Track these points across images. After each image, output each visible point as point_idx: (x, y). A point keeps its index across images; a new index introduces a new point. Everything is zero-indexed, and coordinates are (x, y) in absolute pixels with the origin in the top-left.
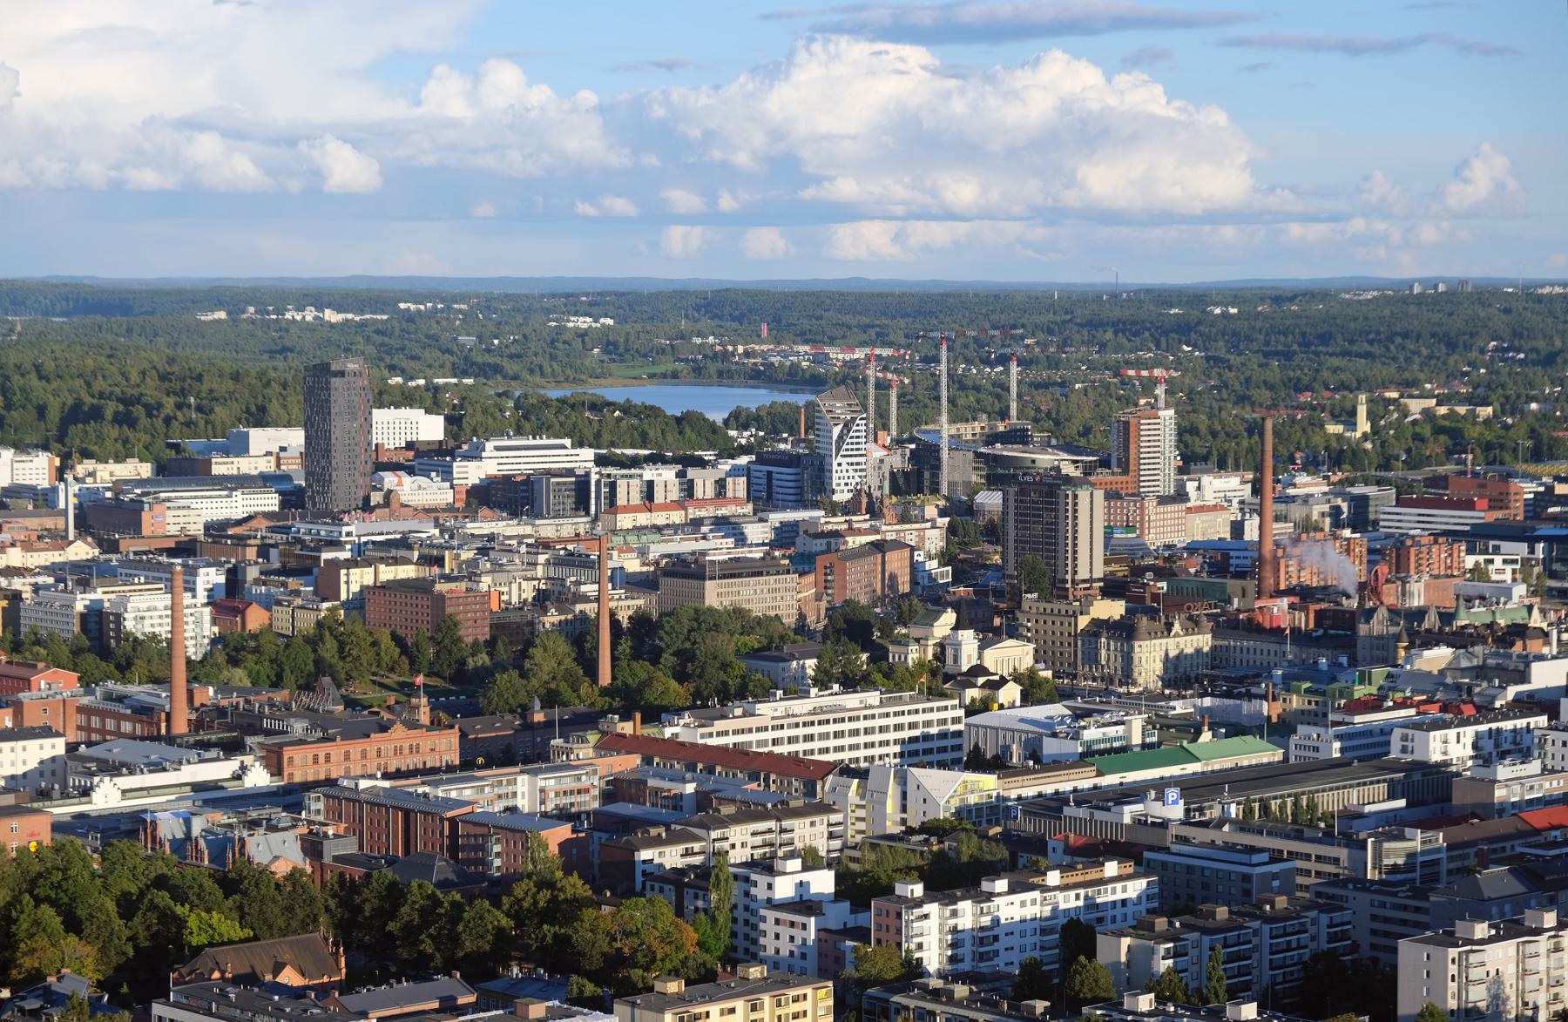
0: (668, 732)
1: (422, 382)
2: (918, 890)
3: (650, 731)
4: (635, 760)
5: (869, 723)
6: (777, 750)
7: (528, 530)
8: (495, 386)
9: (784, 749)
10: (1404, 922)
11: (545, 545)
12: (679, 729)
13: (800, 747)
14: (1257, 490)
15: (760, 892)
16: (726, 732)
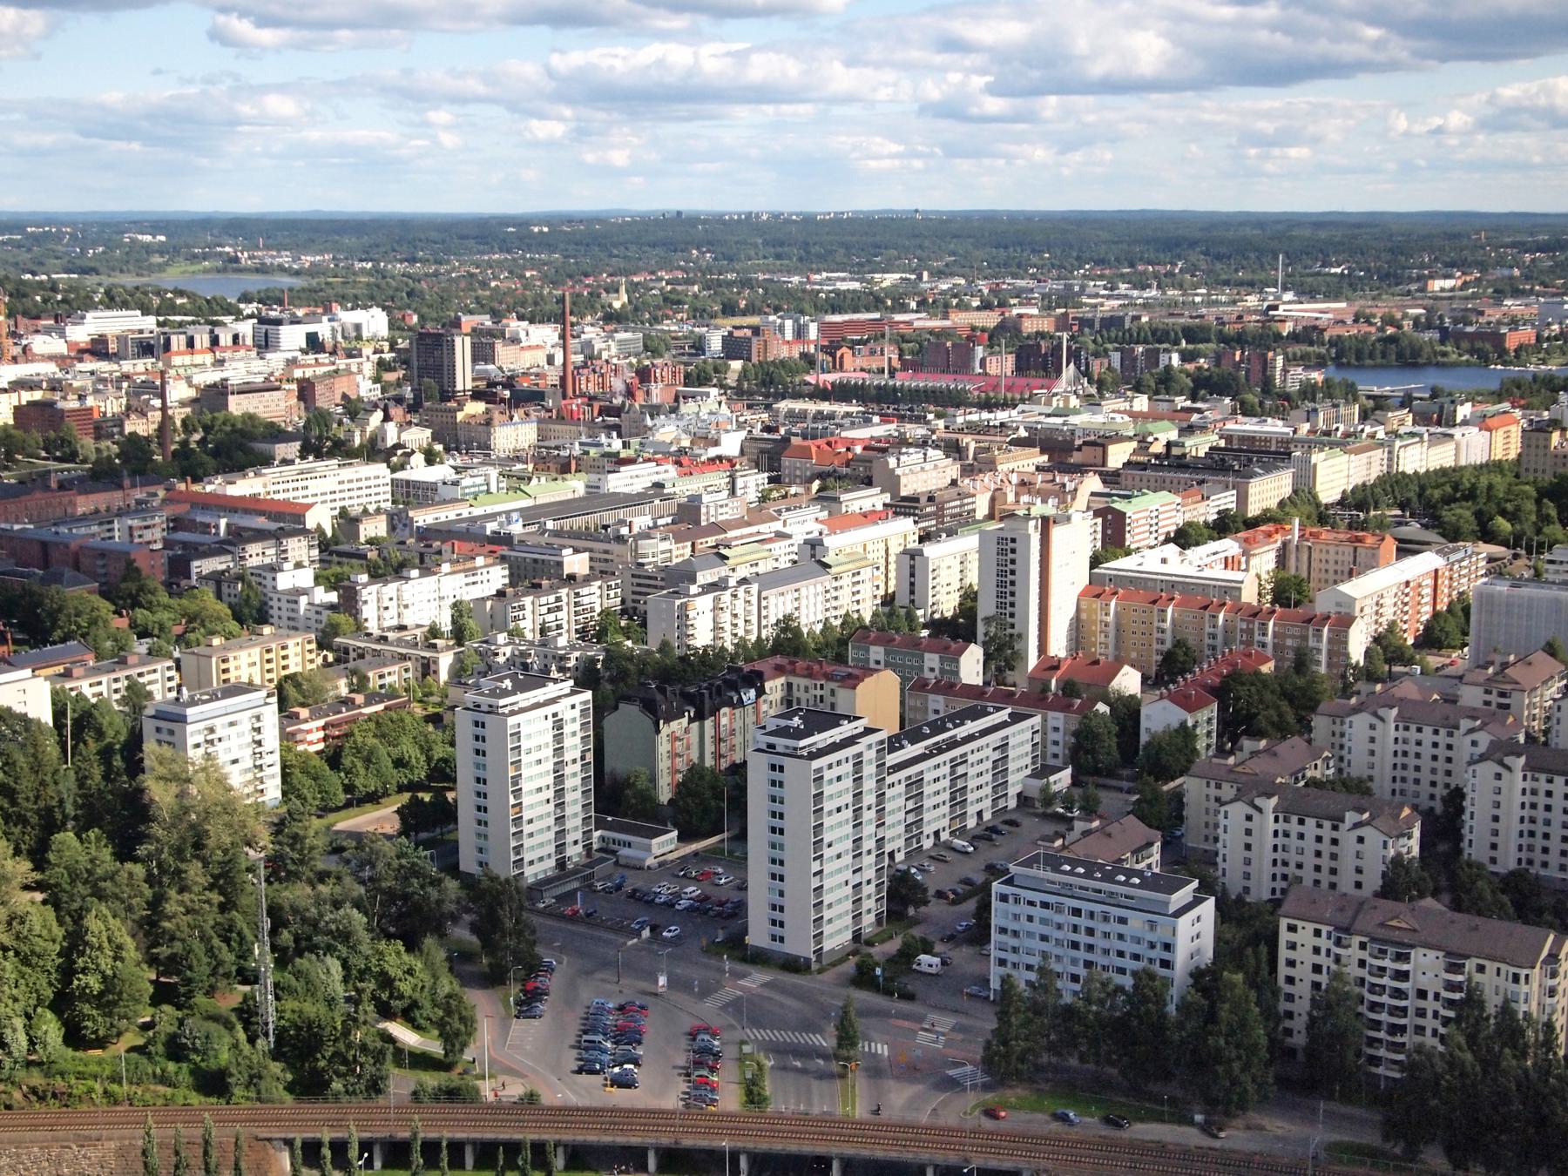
0: (209, 488)
1: (44, 277)
2: (364, 578)
3: (196, 488)
4: (187, 507)
5: (286, 486)
6: (276, 497)
7: (116, 367)
8: (91, 280)
9: (281, 496)
10: (649, 586)
11: (127, 377)
12: (214, 486)
13: (290, 495)
14: (563, 337)
15: (268, 582)
16: (245, 486)
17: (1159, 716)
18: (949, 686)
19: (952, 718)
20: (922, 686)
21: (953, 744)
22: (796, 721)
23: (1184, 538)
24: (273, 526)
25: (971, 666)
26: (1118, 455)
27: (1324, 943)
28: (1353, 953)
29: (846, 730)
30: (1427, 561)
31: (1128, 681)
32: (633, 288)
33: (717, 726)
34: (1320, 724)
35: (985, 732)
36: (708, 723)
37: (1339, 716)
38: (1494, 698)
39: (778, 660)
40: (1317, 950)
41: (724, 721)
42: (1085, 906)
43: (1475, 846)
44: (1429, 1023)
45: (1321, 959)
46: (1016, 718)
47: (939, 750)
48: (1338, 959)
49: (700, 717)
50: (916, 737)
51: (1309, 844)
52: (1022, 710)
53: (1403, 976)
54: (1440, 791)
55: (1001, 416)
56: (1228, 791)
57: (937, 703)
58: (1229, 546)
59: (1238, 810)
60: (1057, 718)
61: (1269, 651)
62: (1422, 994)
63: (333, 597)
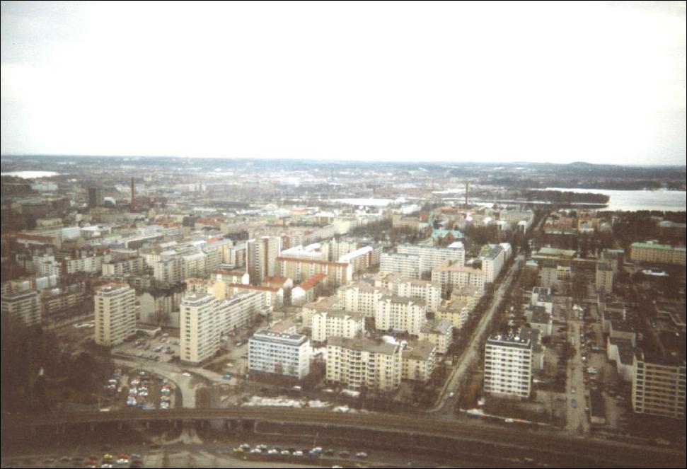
16: (35, 233)
17: (298, 293)
18: (240, 286)
19: (239, 294)
20: (232, 285)
21: (239, 301)
22: (194, 296)
23: (306, 243)
24: (43, 244)
25: (246, 279)
26: (287, 223)
27: (339, 351)
28: (347, 353)
29: (208, 297)
30: (368, 249)
31: (289, 283)
32: (153, 177)
33: (173, 298)
34: (339, 292)
35: (249, 297)
36: (170, 298)
37: (343, 290)
38: (384, 284)
39: (192, 279)
40: (336, 353)
41: (175, 297)
42: (275, 344)
43: (379, 324)
44: (366, 371)
45: (338, 356)
46: (257, 293)
47: (235, 302)
48: (342, 355)
49: (168, 295)
50: (229, 299)
51: (336, 325)
52: (259, 291)
53: (359, 359)
54: (370, 312)
55: (257, 211)
56: (314, 311)
57: (236, 290)
58: (317, 245)
59: (318, 316)
60: (269, 293)
61: (326, 273)
62: (364, 364)
63: (60, 264)
